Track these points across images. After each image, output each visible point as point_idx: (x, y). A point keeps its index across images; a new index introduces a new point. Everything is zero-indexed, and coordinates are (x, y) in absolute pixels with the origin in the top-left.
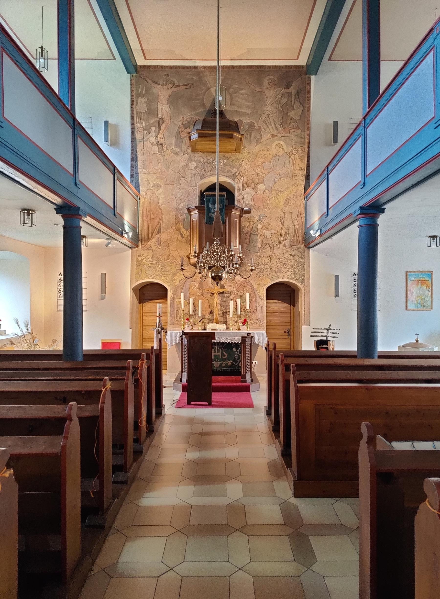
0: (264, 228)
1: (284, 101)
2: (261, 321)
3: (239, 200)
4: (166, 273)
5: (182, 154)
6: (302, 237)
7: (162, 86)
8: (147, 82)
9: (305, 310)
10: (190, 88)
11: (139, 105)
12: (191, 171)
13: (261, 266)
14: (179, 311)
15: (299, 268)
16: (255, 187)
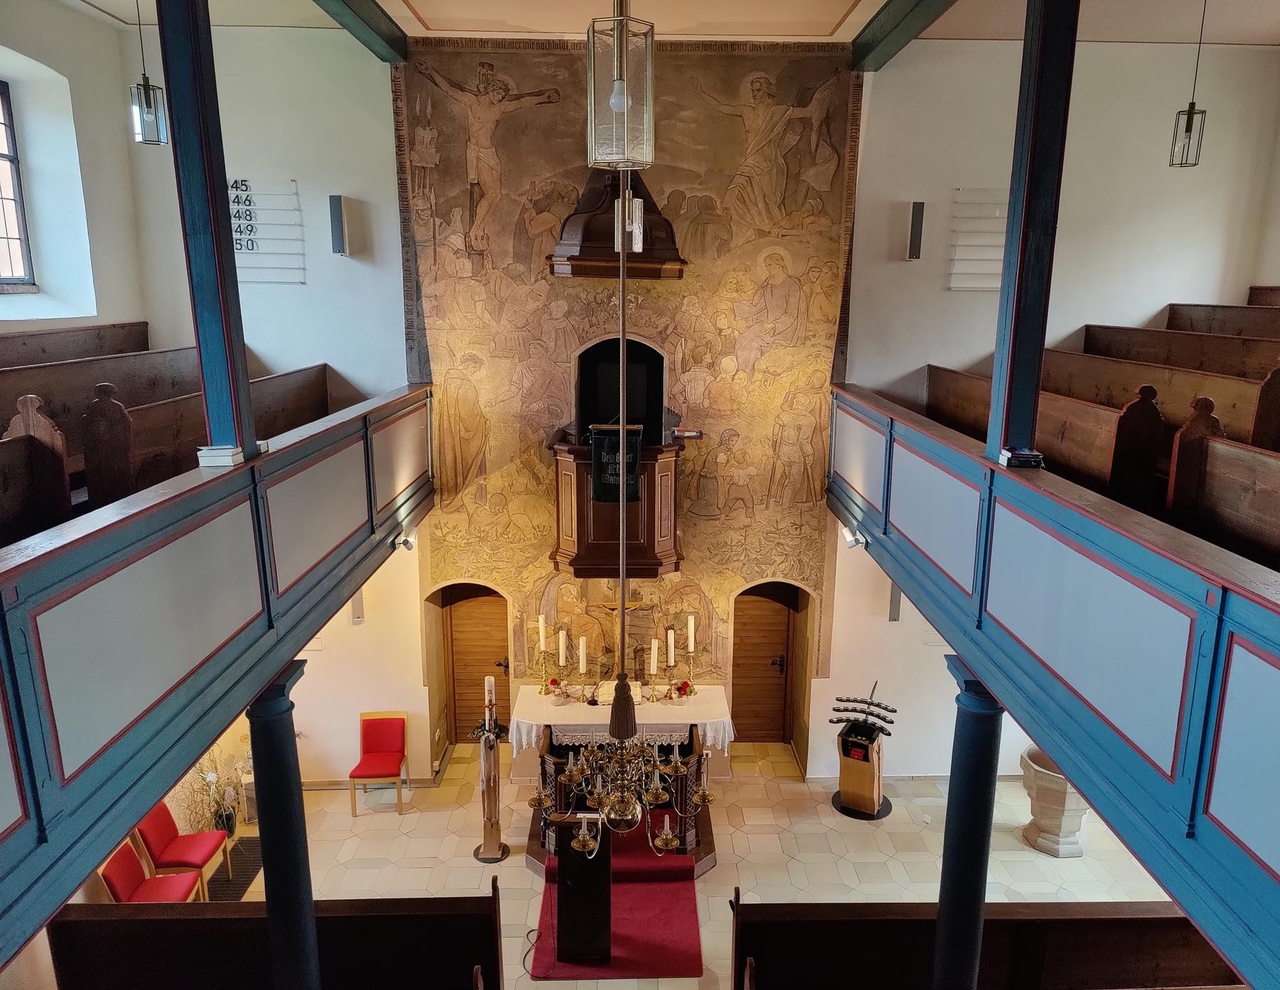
0: (733, 462)
1: (792, 139)
3: (674, 395)
4: (501, 565)
5: (533, 280)
6: (822, 483)
8: (436, 85)
9: (821, 644)
10: (548, 103)
11: (418, 147)
12: (555, 323)
13: (723, 550)
14: (533, 649)
15: (810, 553)
16: (713, 363)
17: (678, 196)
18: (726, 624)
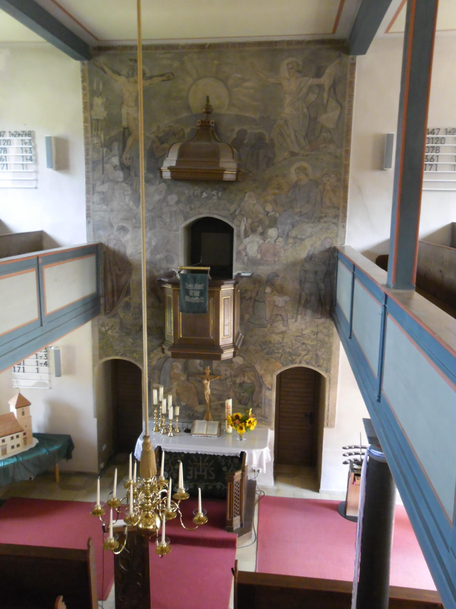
2: (267, 418)
7: (127, 78)
17: (243, 133)
18: (270, 392)
